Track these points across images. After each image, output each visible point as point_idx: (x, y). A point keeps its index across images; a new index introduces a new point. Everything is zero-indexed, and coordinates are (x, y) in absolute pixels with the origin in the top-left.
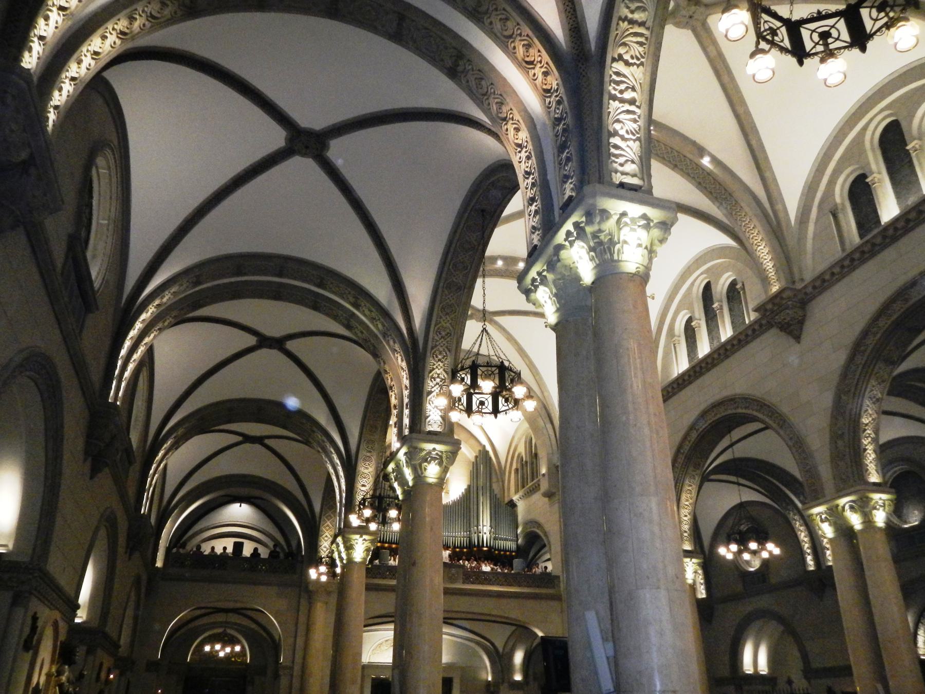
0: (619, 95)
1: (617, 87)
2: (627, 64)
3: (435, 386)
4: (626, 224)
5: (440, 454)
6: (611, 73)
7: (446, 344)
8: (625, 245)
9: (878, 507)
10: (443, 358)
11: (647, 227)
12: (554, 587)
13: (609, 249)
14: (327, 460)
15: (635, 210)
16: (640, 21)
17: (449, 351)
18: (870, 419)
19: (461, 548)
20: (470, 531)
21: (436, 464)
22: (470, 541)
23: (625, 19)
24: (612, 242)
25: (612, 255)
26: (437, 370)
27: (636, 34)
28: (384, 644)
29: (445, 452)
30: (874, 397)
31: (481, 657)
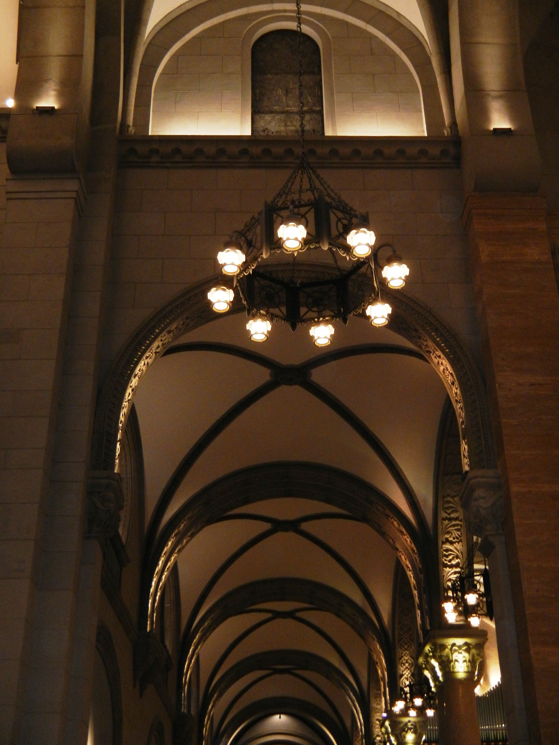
0: (449, 564)
1: (447, 559)
2: (452, 543)
3: (405, 670)
4: (455, 651)
5: (414, 724)
6: (442, 550)
8: (456, 663)
10: (408, 647)
11: (468, 651)
13: (448, 666)
14: (345, 693)
15: (460, 641)
16: (455, 517)
21: (412, 733)
23: (446, 519)
24: (450, 661)
25: (450, 668)
27: (454, 526)
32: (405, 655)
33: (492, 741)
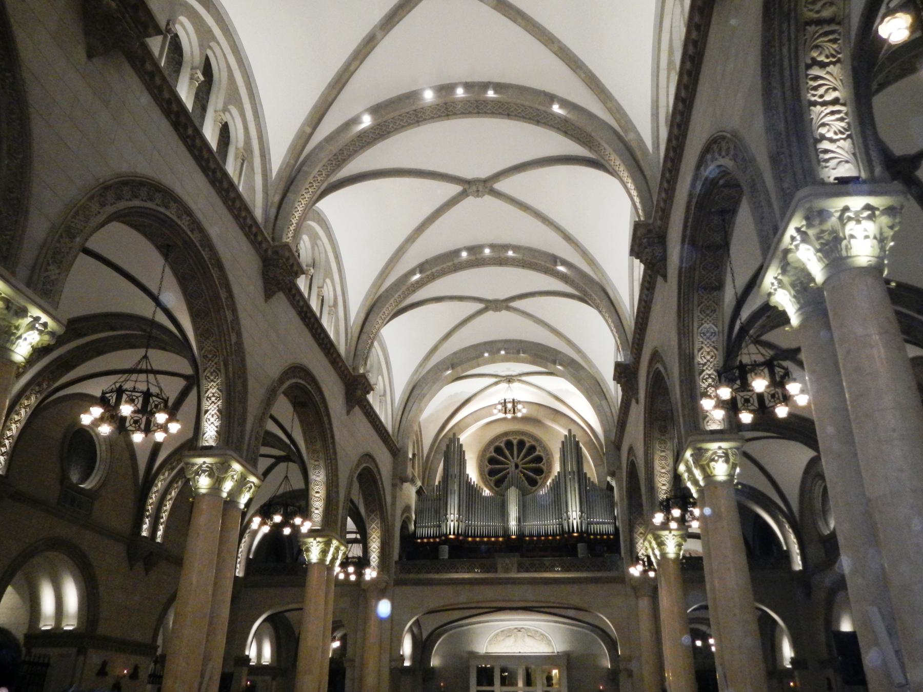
5: (210, 466)
7: (215, 366)
9: (716, 458)
10: (215, 378)
12: (617, 569)
17: (220, 371)
18: (708, 357)
19: (554, 535)
20: (562, 518)
21: (206, 476)
22: (562, 527)
26: (211, 390)
28: (500, 634)
29: (215, 463)
30: (708, 332)
31: (601, 645)
32: (211, 387)
33: (543, 536)
